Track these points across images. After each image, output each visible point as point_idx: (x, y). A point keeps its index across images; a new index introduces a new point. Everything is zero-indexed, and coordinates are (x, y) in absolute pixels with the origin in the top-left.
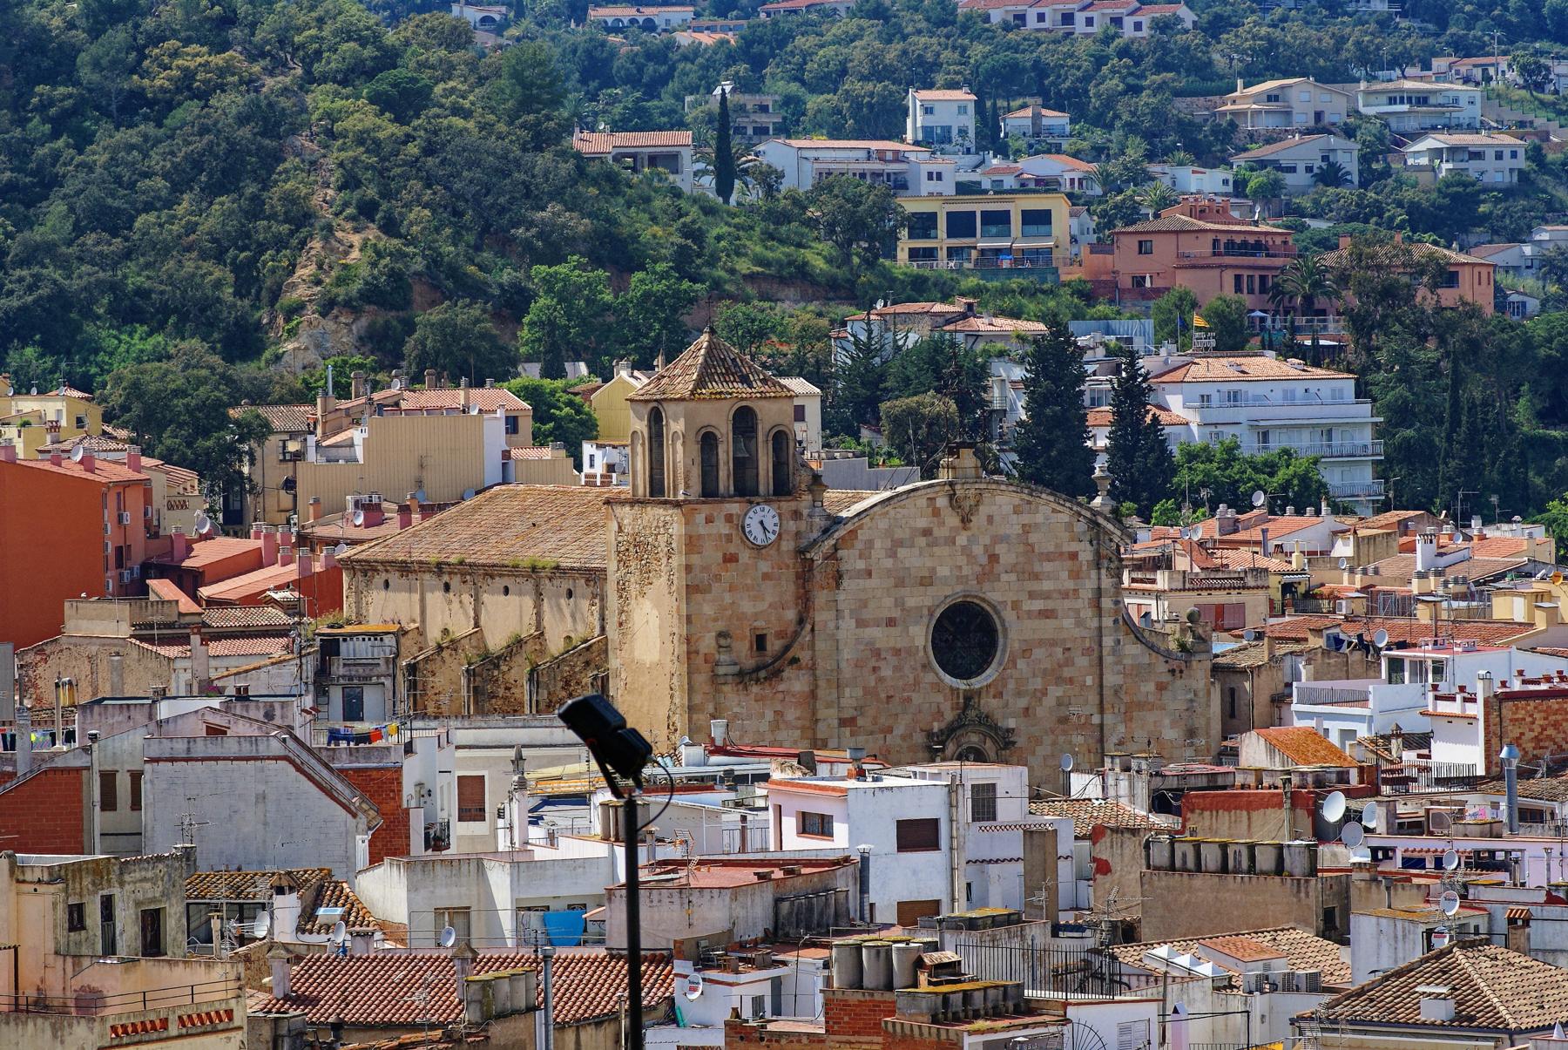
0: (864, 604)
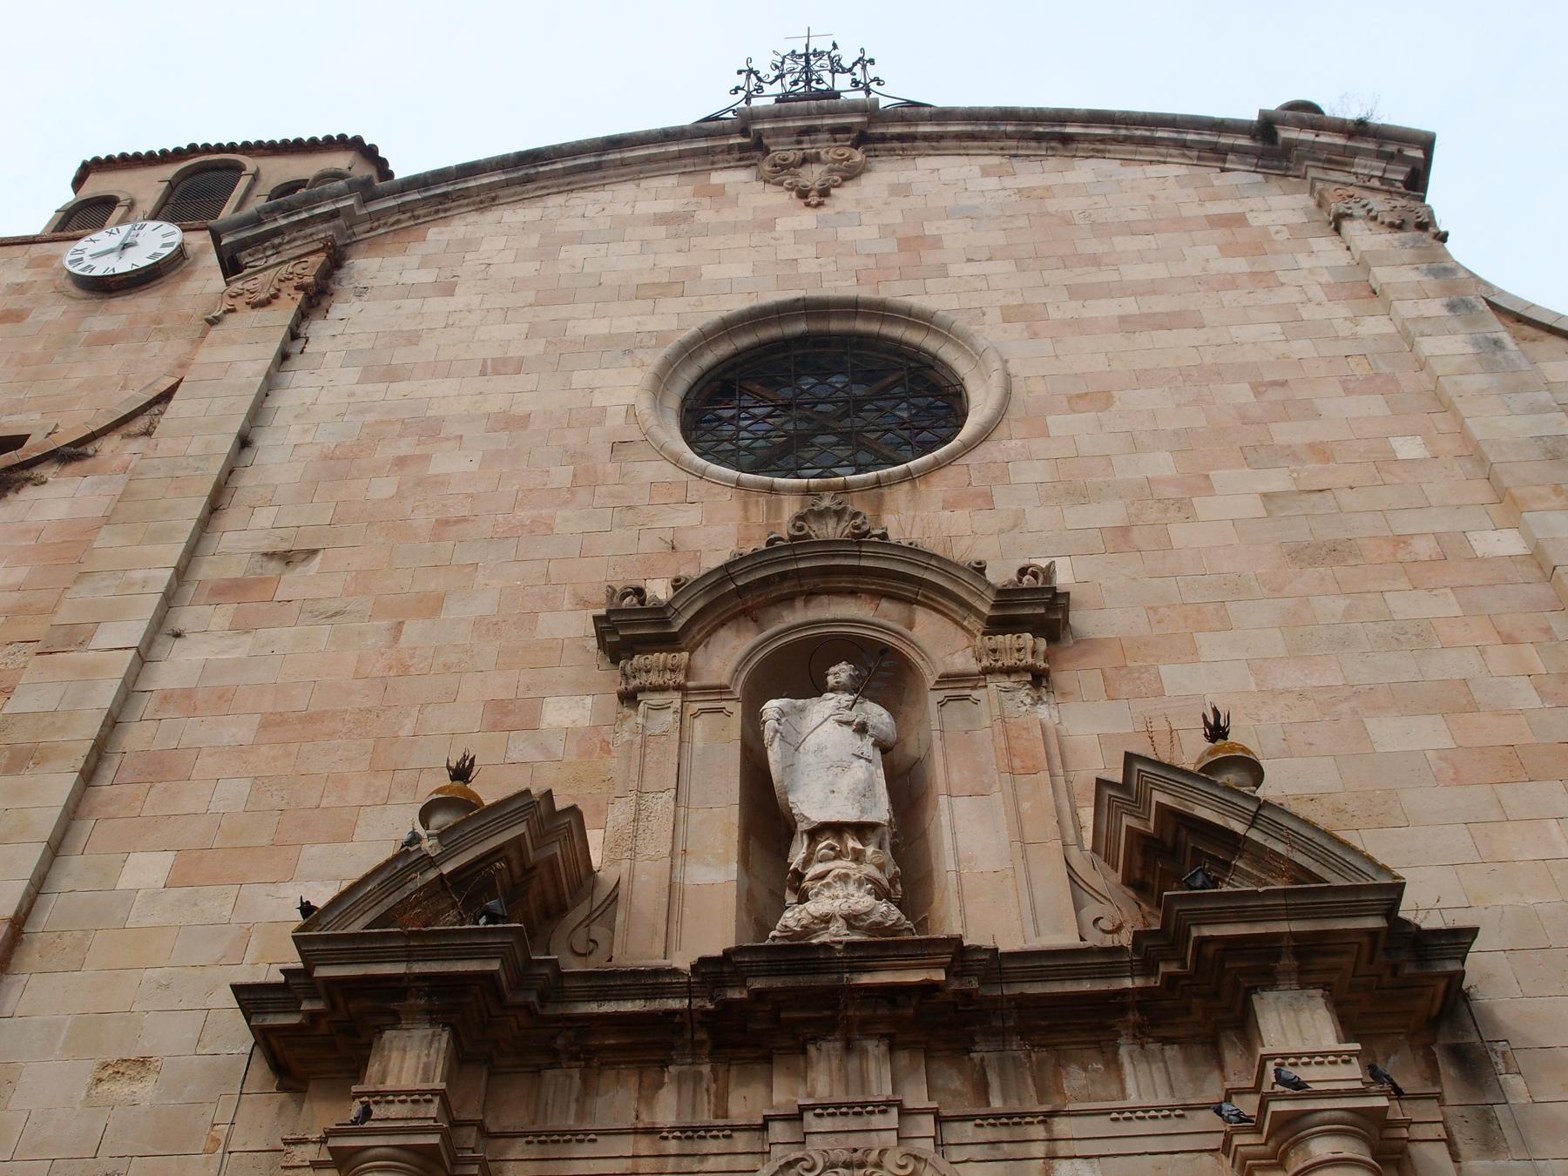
0: (412, 339)
